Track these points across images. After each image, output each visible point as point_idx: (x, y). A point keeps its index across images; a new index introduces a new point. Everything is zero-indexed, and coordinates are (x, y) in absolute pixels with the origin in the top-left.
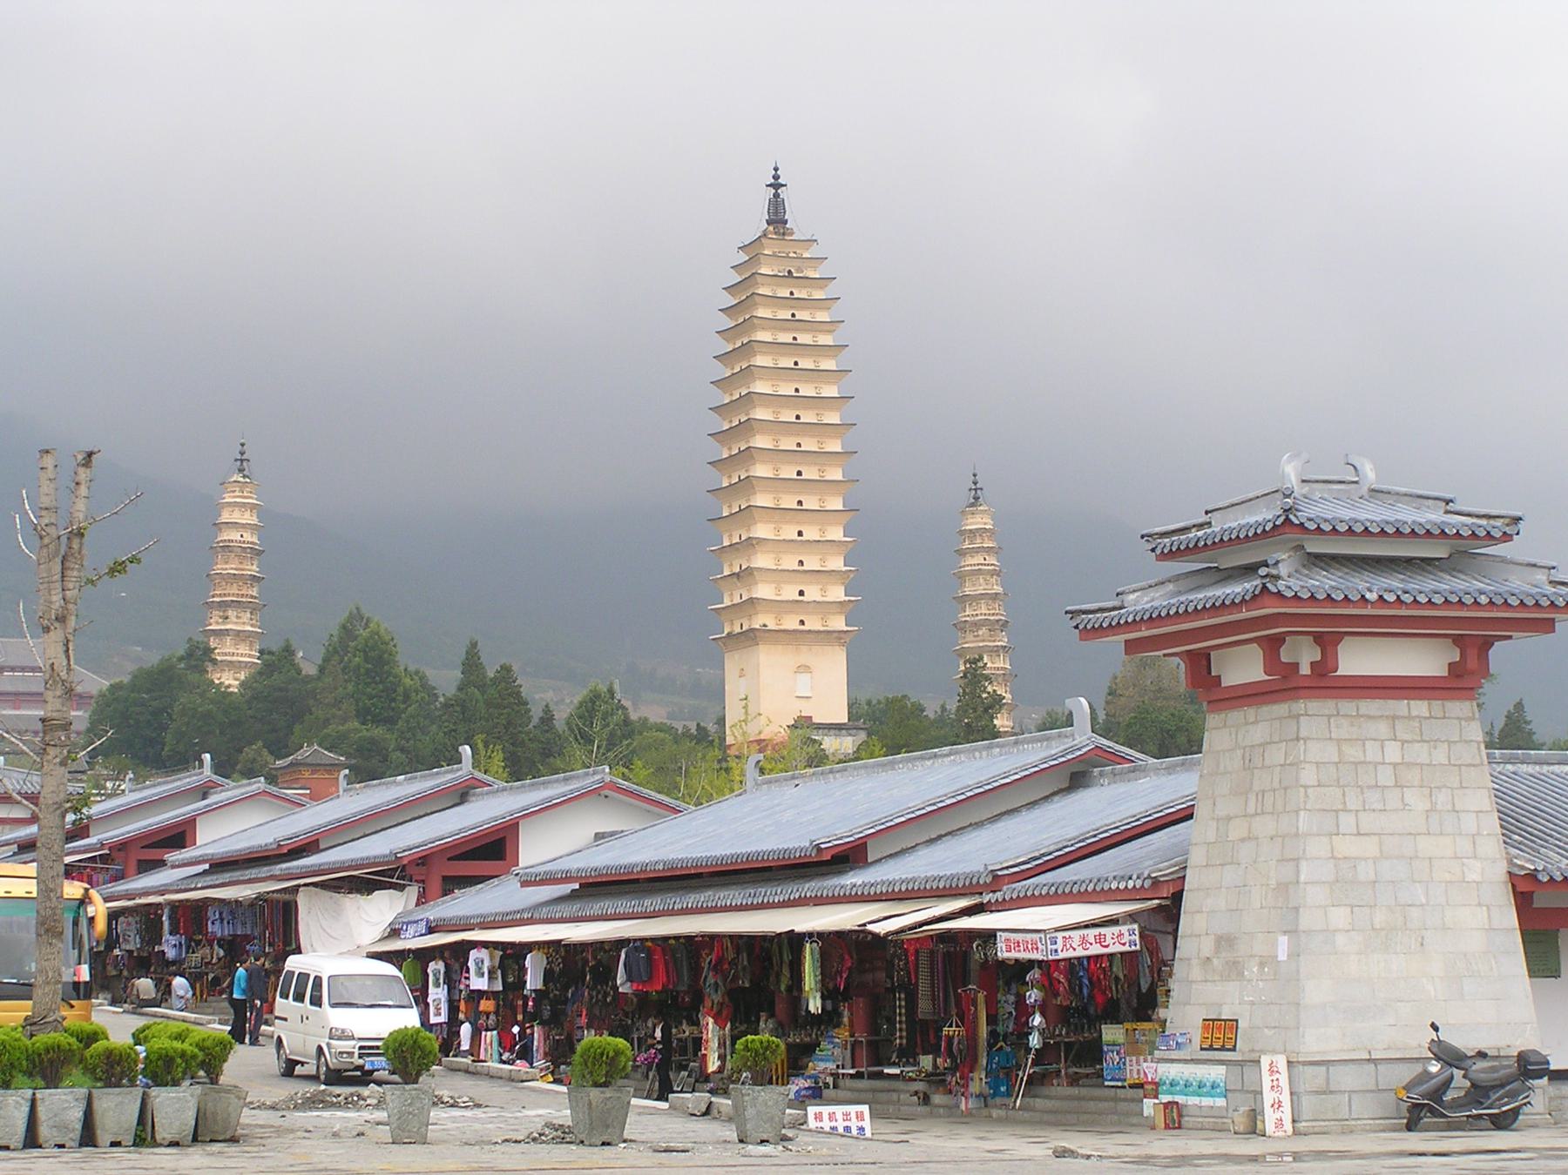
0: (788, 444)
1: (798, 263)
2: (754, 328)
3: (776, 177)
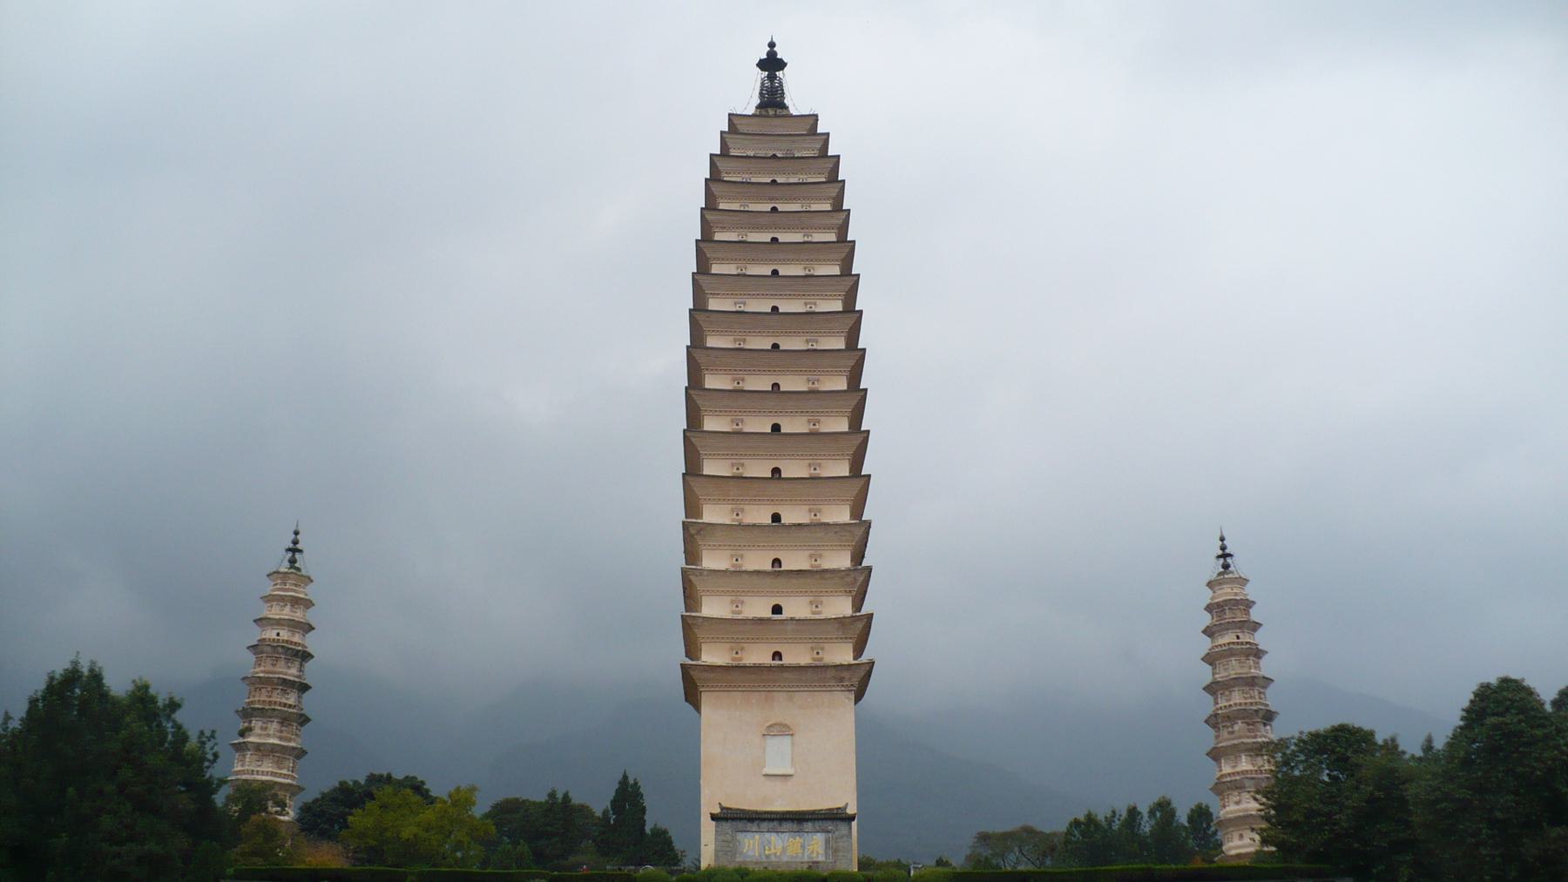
3: (772, 55)
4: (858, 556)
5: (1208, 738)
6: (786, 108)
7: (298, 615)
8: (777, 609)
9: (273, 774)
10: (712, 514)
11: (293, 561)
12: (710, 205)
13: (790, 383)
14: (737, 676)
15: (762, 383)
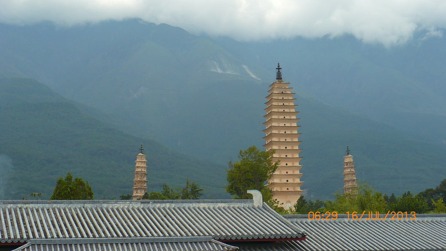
0: (283, 140)
1: (284, 90)
2: (272, 108)
3: (279, 66)
6: (281, 79)
8: (287, 181)
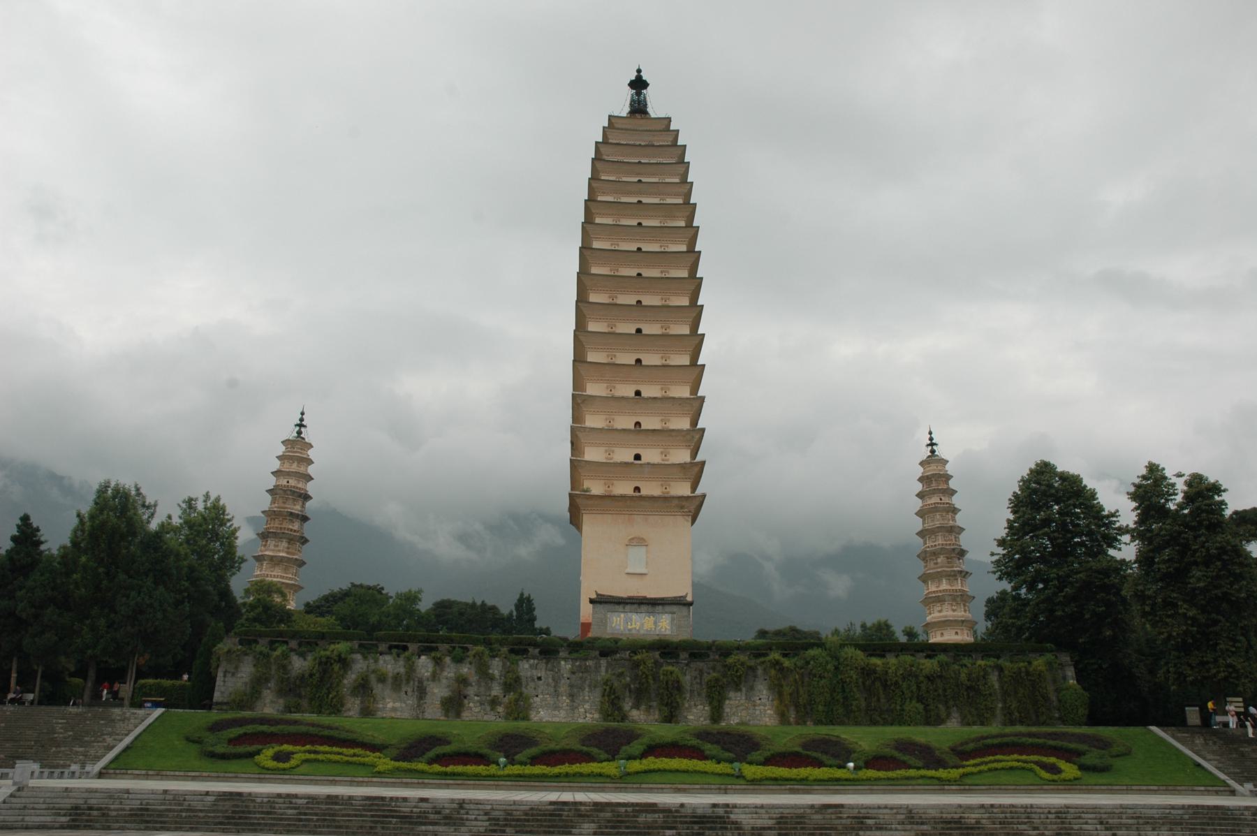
4: (695, 422)
5: (920, 568)
6: (646, 113)
7: (302, 470)
8: (638, 457)
9: (282, 577)
10: (593, 389)
11: (299, 433)
12: (594, 178)
13: (648, 300)
14: (610, 502)
15: (630, 300)
